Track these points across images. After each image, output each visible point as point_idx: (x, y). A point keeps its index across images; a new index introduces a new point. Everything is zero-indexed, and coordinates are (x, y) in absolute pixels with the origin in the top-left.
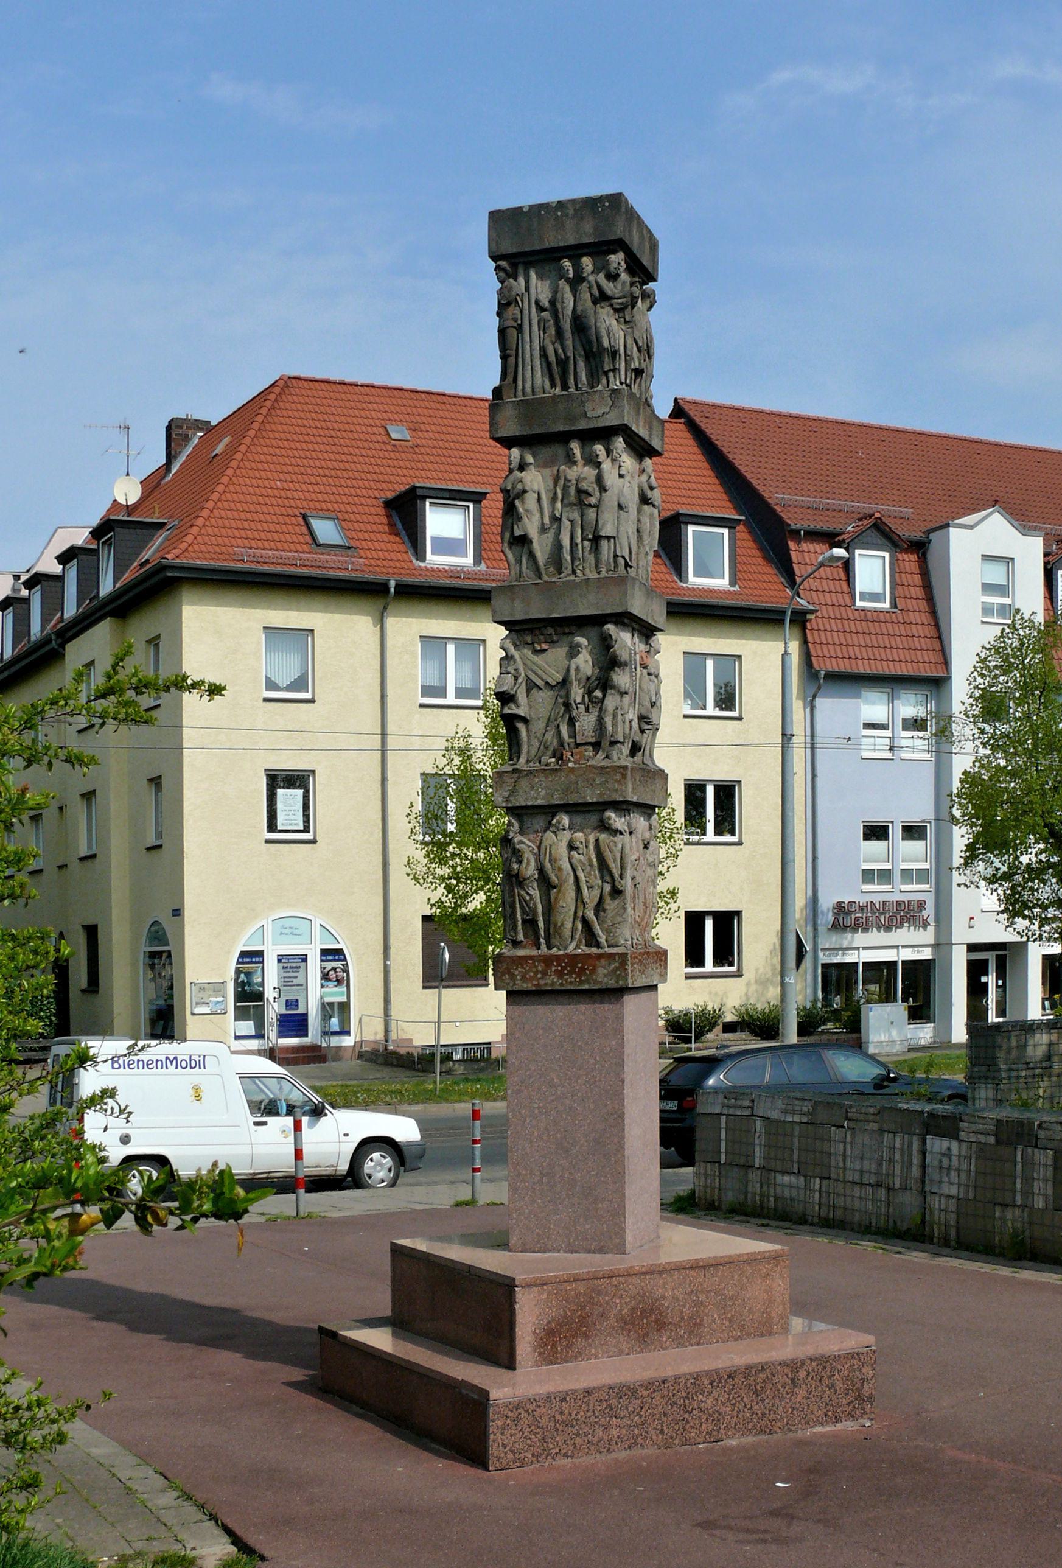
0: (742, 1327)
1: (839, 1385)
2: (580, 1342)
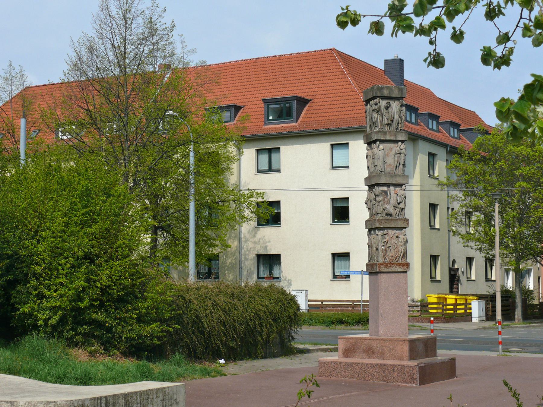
0: (395, 357)
1: (406, 374)
2: (353, 354)
